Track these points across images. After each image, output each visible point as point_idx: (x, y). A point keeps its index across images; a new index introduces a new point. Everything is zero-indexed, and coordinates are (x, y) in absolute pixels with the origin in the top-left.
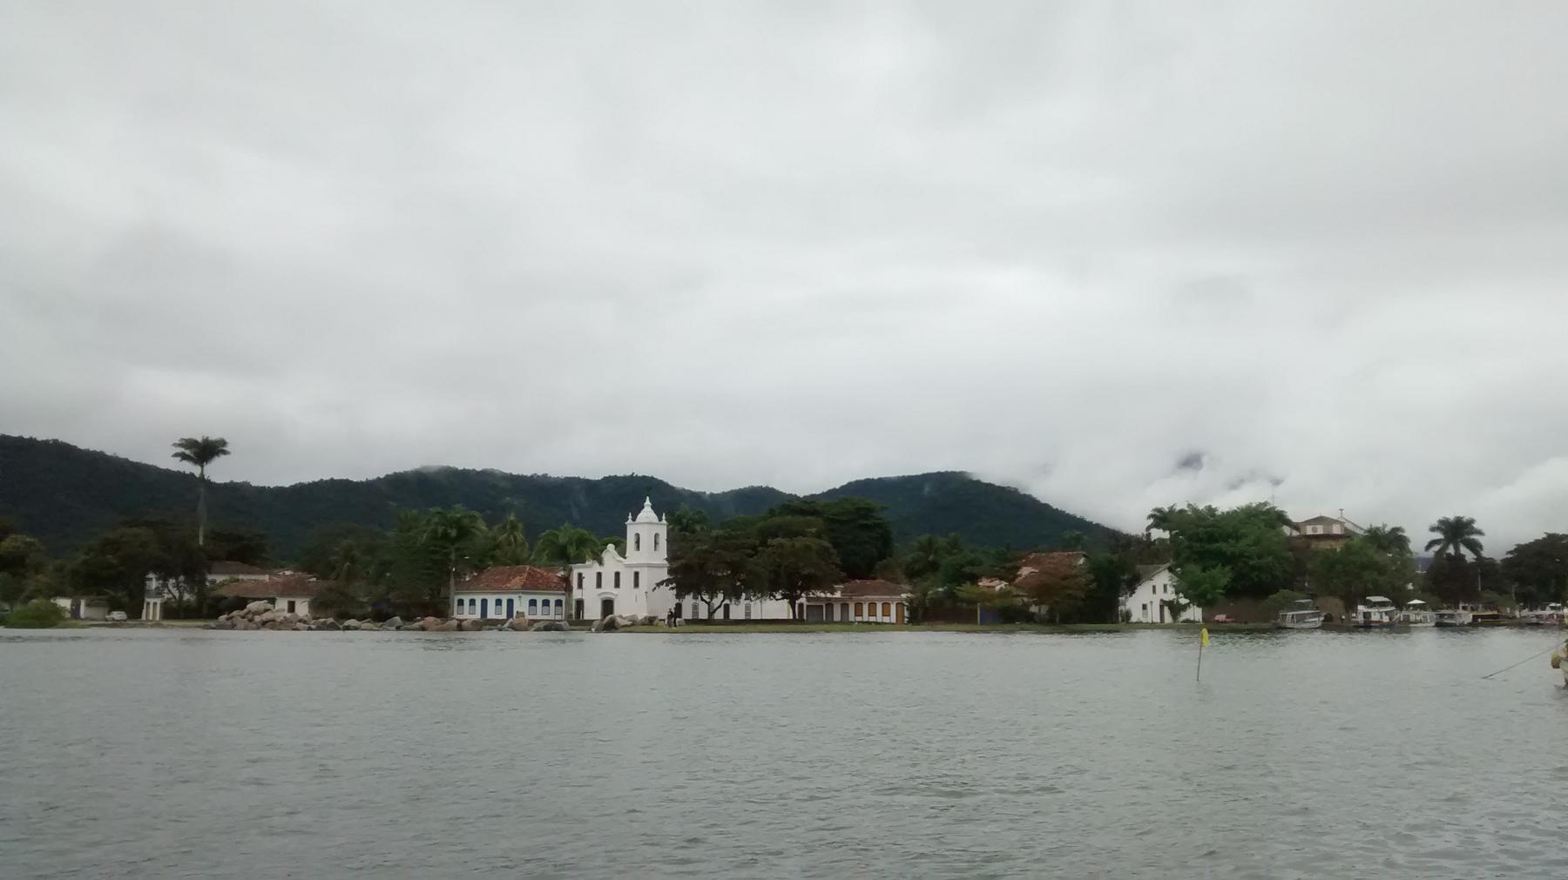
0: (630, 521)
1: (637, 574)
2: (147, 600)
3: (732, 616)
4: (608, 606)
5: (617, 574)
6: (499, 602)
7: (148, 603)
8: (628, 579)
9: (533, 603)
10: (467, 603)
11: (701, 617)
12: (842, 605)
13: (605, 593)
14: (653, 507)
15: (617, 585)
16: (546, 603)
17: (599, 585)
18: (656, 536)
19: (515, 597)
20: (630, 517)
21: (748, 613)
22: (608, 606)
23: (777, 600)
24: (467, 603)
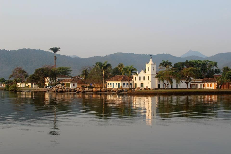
2: (45, 83)
3: (173, 87)
4: (142, 85)
5: (144, 77)
6: (116, 84)
7: (46, 84)
8: (146, 78)
9: (124, 84)
10: (109, 84)
14: (152, 60)
15: (144, 79)
17: (140, 80)
20: (147, 63)
21: (177, 86)
22: (142, 85)
23: (183, 83)
24: (109, 84)
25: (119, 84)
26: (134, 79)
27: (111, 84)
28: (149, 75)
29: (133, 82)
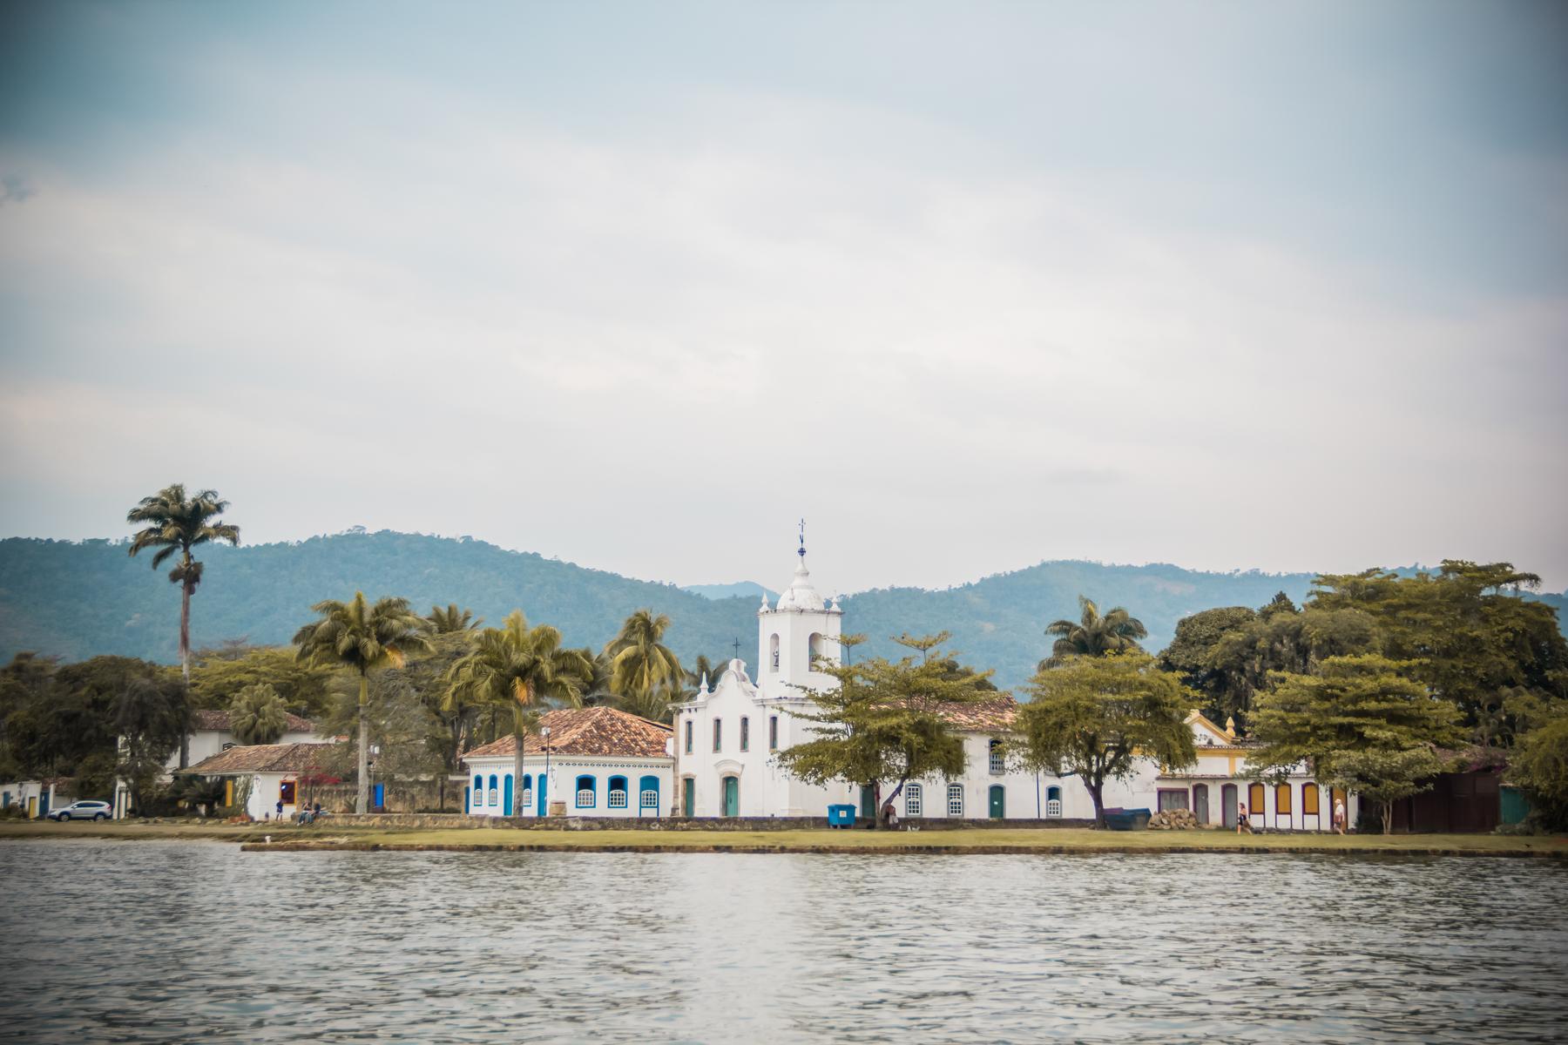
1: (774, 719)
4: (730, 783)
5: (745, 721)
9: (586, 783)
10: (486, 783)
12: (1225, 788)
13: (725, 762)
15: (744, 745)
16: (618, 783)
17: (717, 748)
22: (730, 783)
24: (486, 783)
26: (676, 743)
27: (493, 780)
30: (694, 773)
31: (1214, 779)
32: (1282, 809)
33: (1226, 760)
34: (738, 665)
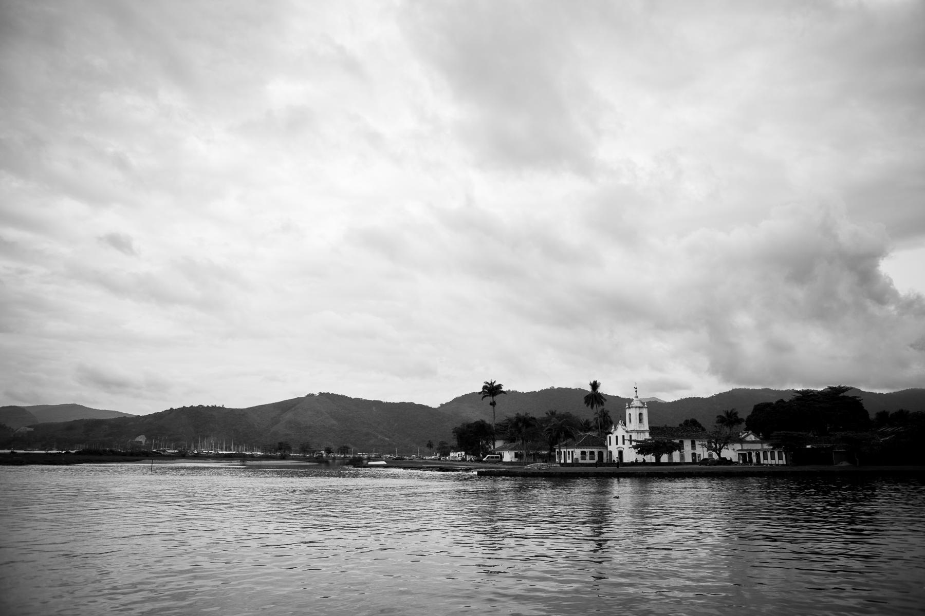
0: (627, 406)
4: (621, 453)
5: (623, 436)
9: (583, 453)
11: (686, 461)
13: (619, 447)
17: (617, 444)
18: (640, 415)
19: (573, 450)
20: (627, 404)
22: (621, 453)
25: (572, 452)
28: (632, 431)
29: (607, 447)
30: (611, 450)
31: (753, 450)
32: (773, 458)
33: (760, 445)
34: (622, 422)
